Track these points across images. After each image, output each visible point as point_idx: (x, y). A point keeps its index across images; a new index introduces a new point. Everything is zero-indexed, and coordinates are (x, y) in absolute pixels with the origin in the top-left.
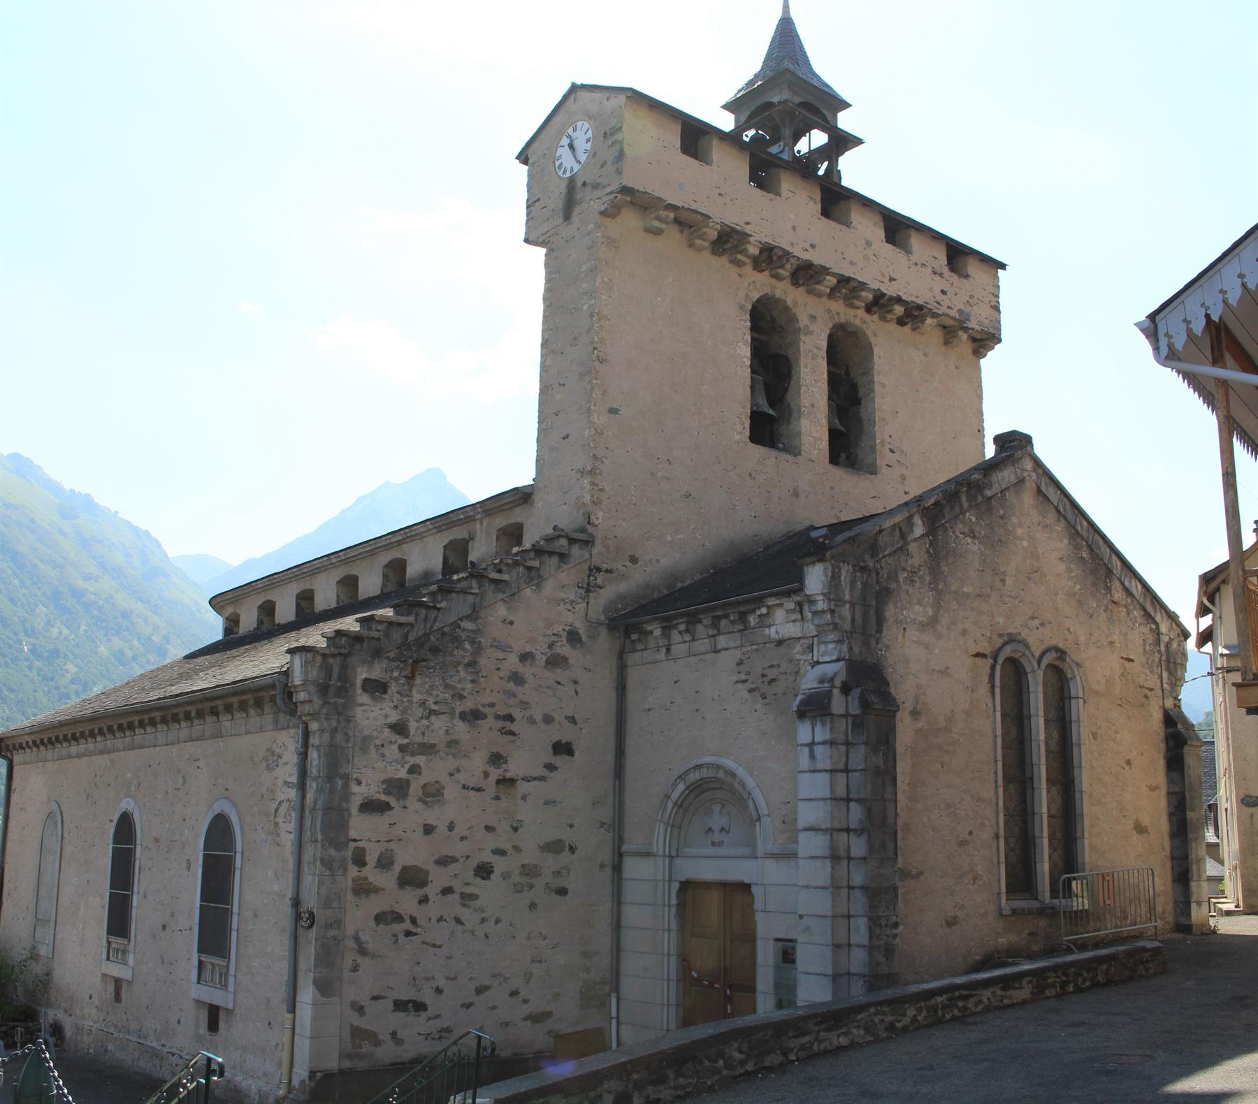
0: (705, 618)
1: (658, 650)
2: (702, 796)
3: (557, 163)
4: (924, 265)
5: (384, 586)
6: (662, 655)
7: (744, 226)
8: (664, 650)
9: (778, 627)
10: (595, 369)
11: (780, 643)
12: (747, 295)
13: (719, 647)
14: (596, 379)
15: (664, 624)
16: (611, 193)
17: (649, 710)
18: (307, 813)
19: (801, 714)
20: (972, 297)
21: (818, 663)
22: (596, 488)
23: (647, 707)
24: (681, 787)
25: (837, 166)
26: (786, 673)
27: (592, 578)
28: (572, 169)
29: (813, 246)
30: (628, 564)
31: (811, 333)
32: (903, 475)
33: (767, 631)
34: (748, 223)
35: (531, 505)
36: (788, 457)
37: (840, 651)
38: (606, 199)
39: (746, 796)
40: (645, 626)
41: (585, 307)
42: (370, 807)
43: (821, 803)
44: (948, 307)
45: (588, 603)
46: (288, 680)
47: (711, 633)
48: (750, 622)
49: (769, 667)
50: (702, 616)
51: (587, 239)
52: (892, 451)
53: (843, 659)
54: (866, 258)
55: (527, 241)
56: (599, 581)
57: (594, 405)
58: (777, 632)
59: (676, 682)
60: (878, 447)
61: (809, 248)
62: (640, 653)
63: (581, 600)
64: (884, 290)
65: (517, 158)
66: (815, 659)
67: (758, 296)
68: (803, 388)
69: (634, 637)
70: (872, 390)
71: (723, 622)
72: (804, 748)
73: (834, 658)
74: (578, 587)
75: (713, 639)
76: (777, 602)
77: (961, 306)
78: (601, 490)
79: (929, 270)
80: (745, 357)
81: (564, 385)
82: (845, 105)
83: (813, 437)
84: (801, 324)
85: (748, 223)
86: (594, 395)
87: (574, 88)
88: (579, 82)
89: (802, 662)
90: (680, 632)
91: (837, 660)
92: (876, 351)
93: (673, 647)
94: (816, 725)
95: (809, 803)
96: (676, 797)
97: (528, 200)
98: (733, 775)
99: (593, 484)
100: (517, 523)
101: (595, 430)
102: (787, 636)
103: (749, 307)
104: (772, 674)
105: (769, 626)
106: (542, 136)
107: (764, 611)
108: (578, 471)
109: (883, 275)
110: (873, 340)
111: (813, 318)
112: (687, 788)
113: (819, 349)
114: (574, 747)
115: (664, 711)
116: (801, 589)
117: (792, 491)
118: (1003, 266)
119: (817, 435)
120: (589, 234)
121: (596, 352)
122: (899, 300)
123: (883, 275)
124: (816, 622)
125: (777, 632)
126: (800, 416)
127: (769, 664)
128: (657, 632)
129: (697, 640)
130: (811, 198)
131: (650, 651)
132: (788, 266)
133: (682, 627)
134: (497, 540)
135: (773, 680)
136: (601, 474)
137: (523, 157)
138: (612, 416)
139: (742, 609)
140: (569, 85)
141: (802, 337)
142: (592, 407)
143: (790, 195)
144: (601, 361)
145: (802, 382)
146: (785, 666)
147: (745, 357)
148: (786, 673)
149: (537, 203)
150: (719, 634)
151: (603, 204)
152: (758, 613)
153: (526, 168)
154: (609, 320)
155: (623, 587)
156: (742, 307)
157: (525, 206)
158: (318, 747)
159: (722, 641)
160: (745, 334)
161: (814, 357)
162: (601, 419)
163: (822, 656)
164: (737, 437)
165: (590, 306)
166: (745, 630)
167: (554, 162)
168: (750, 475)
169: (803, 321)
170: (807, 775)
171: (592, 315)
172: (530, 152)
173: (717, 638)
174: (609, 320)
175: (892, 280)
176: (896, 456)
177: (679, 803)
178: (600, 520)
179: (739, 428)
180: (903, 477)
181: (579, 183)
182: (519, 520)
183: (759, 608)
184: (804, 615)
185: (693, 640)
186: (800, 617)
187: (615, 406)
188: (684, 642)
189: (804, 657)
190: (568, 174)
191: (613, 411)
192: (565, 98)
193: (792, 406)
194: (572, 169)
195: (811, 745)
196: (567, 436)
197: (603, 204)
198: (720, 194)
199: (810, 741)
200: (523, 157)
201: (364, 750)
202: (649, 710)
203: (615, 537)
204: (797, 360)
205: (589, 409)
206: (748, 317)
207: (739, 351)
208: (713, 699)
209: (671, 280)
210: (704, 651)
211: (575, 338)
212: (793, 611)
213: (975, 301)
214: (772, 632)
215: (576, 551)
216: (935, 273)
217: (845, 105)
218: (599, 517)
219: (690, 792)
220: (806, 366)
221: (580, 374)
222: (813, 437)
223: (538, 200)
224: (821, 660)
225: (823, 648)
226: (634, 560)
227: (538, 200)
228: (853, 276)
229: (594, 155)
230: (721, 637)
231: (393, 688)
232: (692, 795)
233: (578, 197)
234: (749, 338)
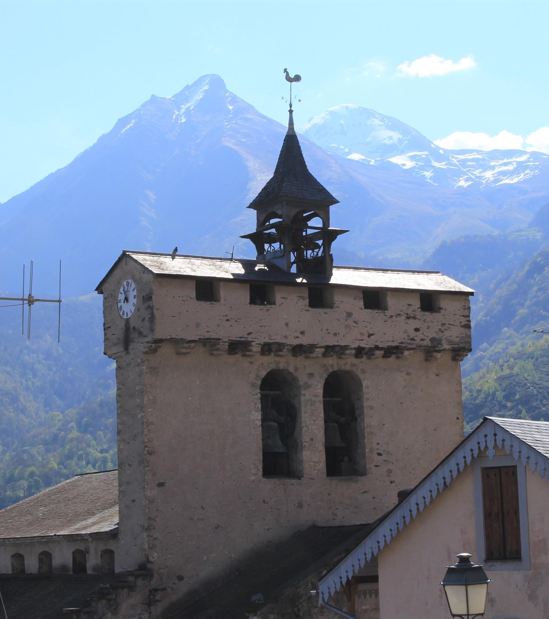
4: (399, 315)
5: (40, 567)
7: (247, 336)
10: (146, 461)
12: (257, 375)
14: (148, 466)
16: (148, 342)
20: (443, 324)
22: (152, 538)
25: (330, 251)
27: (152, 596)
29: (302, 333)
30: (177, 581)
31: (310, 387)
32: (389, 470)
34: (250, 334)
36: (294, 481)
41: (139, 416)
45: (150, 613)
51: (137, 369)
52: (380, 454)
54: (347, 327)
56: (157, 598)
57: (147, 485)
60: (367, 455)
61: (300, 335)
63: (145, 612)
64: (363, 345)
67: (266, 374)
68: (304, 429)
74: (143, 604)
77: (434, 335)
78: (155, 539)
79: (404, 317)
80: (257, 420)
83: (313, 462)
84: (301, 383)
85: (250, 334)
86: (147, 478)
92: (364, 384)
99: (149, 536)
101: (149, 500)
103: (259, 383)
106: (110, 280)
110: (361, 376)
111: (311, 375)
113: (316, 396)
117: (297, 505)
119: (316, 460)
120: (138, 365)
121: (146, 448)
122: (377, 348)
123: (362, 334)
130: (300, 297)
134: (101, 558)
136: (154, 528)
137: (100, 289)
138: (161, 488)
141: (303, 392)
142: (146, 486)
143: (283, 300)
144: (150, 453)
145: (303, 424)
147: (257, 420)
153: (101, 296)
154: (154, 424)
155: (174, 598)
156: (253, 385)
160: (256, 404)
161: (313, 403)
164: (253, 478)
165: (142, 416)
167: (117, 304)
168: (264, 501)
169: (302, 379)
171: (143, 423)
174: (154, 424)
175: (370, 335)
176: (384, 457)
178: (155, 558)
179: (254, 471)
180: (390, 471)
187: (162, 481)
190: (125, 317)
191: (161, 485)
194: (127, 315)
198: (228, 320)
200: (100, 289)
203: (166, 566)
204: (300, 408)
205: (144, 487)
206: (259, 391)
207: (252, 417)
209: (198, 383)
213: (446, 327)
215: (140, 582)
216: (408, 318)
217: (334, 201)
218: (155, 556)
220: (306, 412)
222: (313, 462)
226: (180, 578)
228: (336, 344)
233: (132, 336)
234: (259, 405)
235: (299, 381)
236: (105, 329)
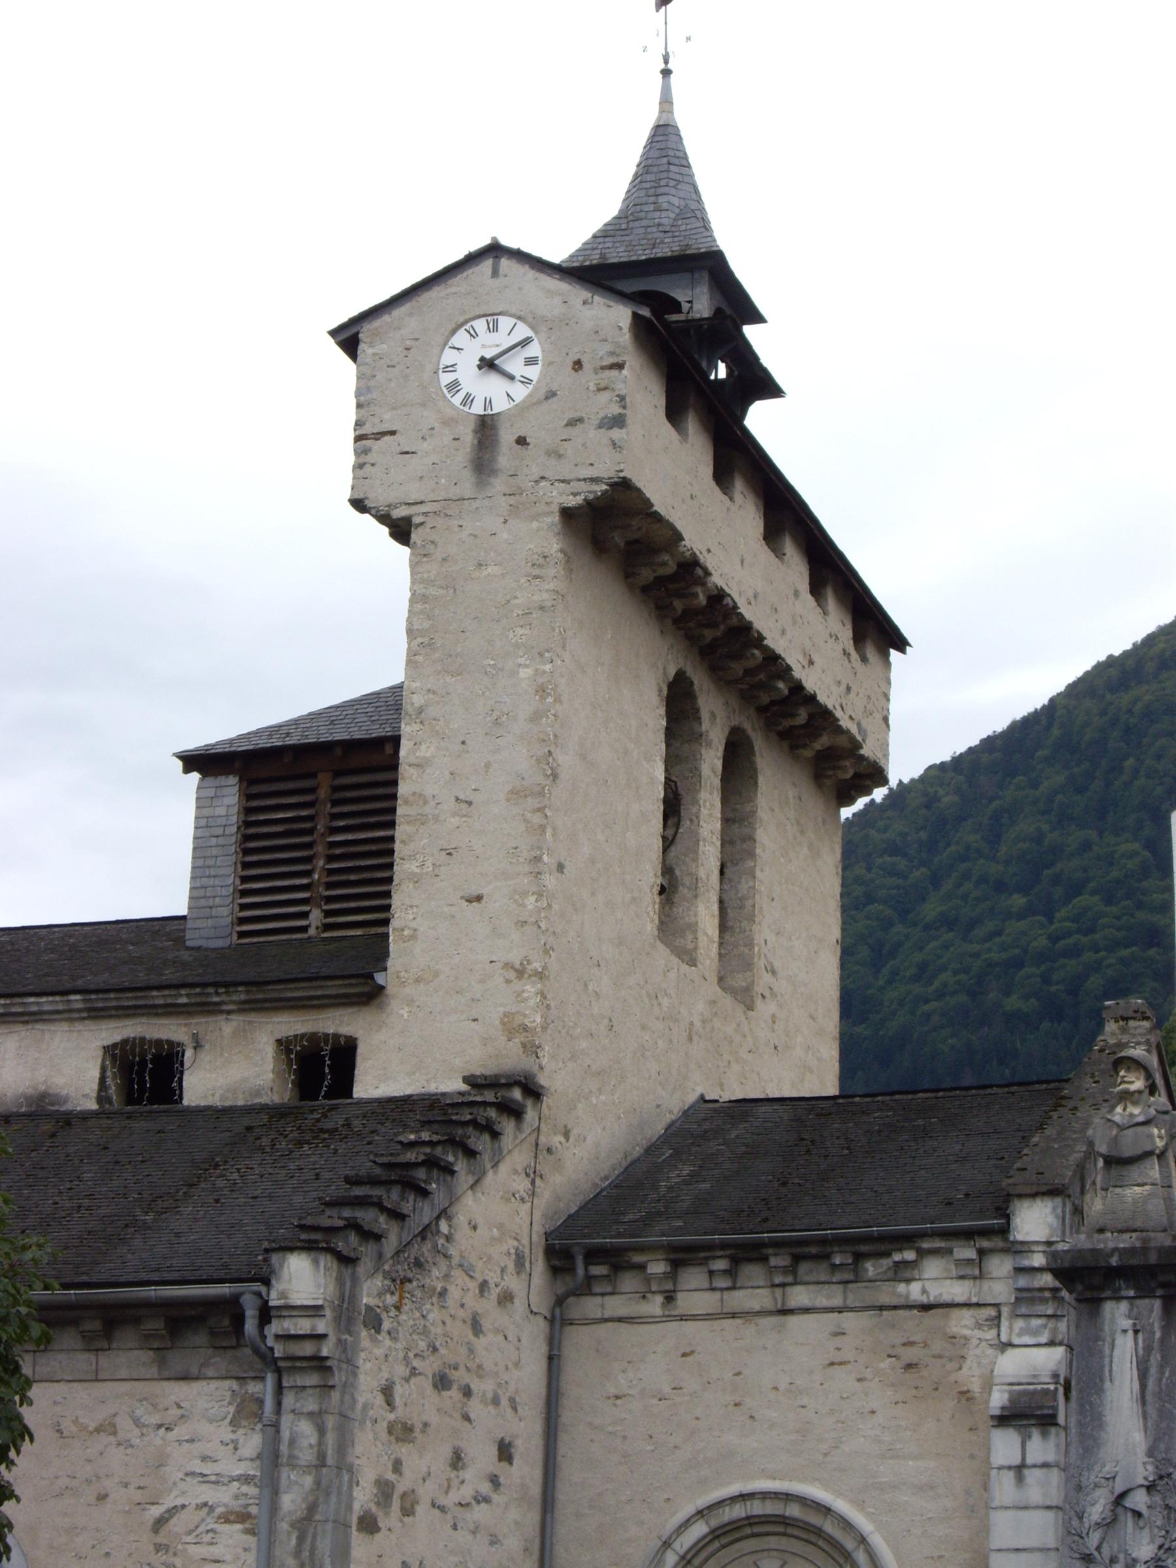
0: (776, 1255)
1: (644, 1297)
2: (737, 1546)
3: (445, 379)
6: (655, 1306)
8: (659, 1299)
9: (928, 1285)
11: (926, 1308)
13: (792, 1303)
15: (672, 1256)
16: (593, 480)
17: (617, 1397)
18: (284, 1526)
19: (1004, 1419)
21: (1010, 1345)
23: (613, 1391)
24: (700, 1529)
26: (940, 1357)
28: (488, 403)
33: (902, 1288)
35: (381, 1007)
37: (1054, 1331)
38: (583, 487)
39: (849, 1544)
40: (630, 1254)
41: (525, 673)
42: (369, 1525)
43: (1038, 1554)
44: (851, 718)
46: (268, 1295)
47: (778, 1280)
48: (867, 1270)
49: (904, 1345)
50: (770, 1251)
53: (1061, 1344)
55: (359, 505)
58: (924, 1291)
59: (684, 1355)
62: (599, 1300)
65: (333, 333)
66: (1004, 1338)
69: (598, 1270)
70: (752, 855)
71: (804, 1268)
72: (1005, 1471)
73: (1043, 1339)
75: (778, 1291)
76: (943, 1245)
81: (470, 803)
82: (756, 317)
87: (494, 250)
88: (506, 242)
89: (975, 1342)
90: (711, 1273)
91: (1051, 1343)
92: (761, 780)
93: (680, 1295)
94: (1030, 1437)
95: (1012, 1556)
96: (686, 1546)
97: (358, 424)
98: (826, 1510)
100: (336, 1036)
102: (946, 1298)
104: (910, 1355)
105: (908, 1281)
106: (398, 312)
107: (910, 1255)
108: (508, 966)
109: (805, 654)
112: (712, 1531)
114: (513, 1450)
115: (655, 1401)
116: (1004, 1231)
118: (901, 644)
124: (1023, 1282)
125: (924, 1291)
126: (696, 897)
127: (904, 1340)
128: (658, 1268)
129: (740, 1288)
131: (624, 1297)
132: (722, 627)
133: (720, 1265)
135: (909, 1366)
139: (864, 1248)
140: (485, 242)
142: (545, 858)
146: (937, 1346)
148: (940, 1357)
149: (387, 438)
150: (795, 1283)
151: (575, 494)
152: (897, 1257)
157: (351, 435)
158: (316, 1418)
159: (799, 1296)
162: (550, 881)
163: (1020, 1335)
166: (856, 1282)
170: (1011, 1513)
172: (366, 332)
173: (789, 1289)
177: (689, 1557)
178: (546, 1060)
181: (506, 437)
182: (345, 1030)
183: (900, 1250)
184: (984, 1269)
185: (733, 1288)
186: (977, 1272)
188: (713, 1289)
189: (977, 1333)
190: (478, 409)
192: (472, 259)
193: (677, 872)
195: (1019, 1469)
196: (479, 898)
197: (575, 494)
199: (1017, 1461)
201: (362, 1423)
202: (617, 1397)
205: (538, 859)
208: (776, 1388)
210: (757, 1308)
211: (497, 722)
212: (969, 1261)
214: (915, 1291)
219: (716, 1534)
221: (511, 792)
223: (393, 433)
224: (1016, 1341)
225: (1019, 1324)
227: (393, 433)
229: (550, 395)
230: (798, 1289)
231: (386, 1325)
232: (716, 1544)
235: (700, 724)
236: (358, 439)
